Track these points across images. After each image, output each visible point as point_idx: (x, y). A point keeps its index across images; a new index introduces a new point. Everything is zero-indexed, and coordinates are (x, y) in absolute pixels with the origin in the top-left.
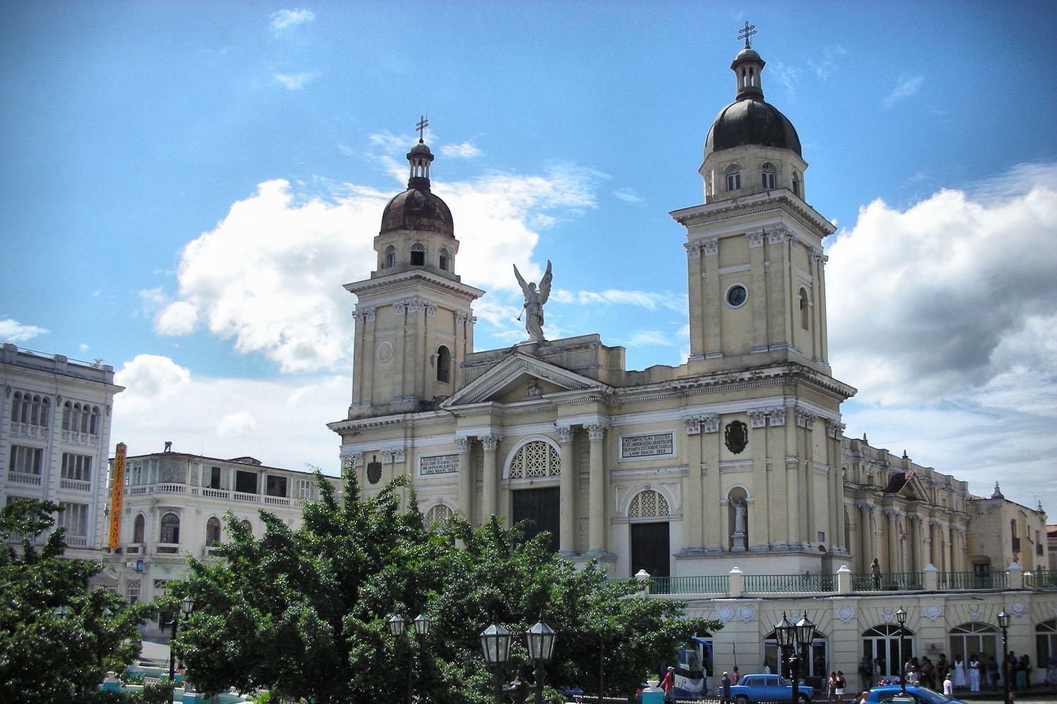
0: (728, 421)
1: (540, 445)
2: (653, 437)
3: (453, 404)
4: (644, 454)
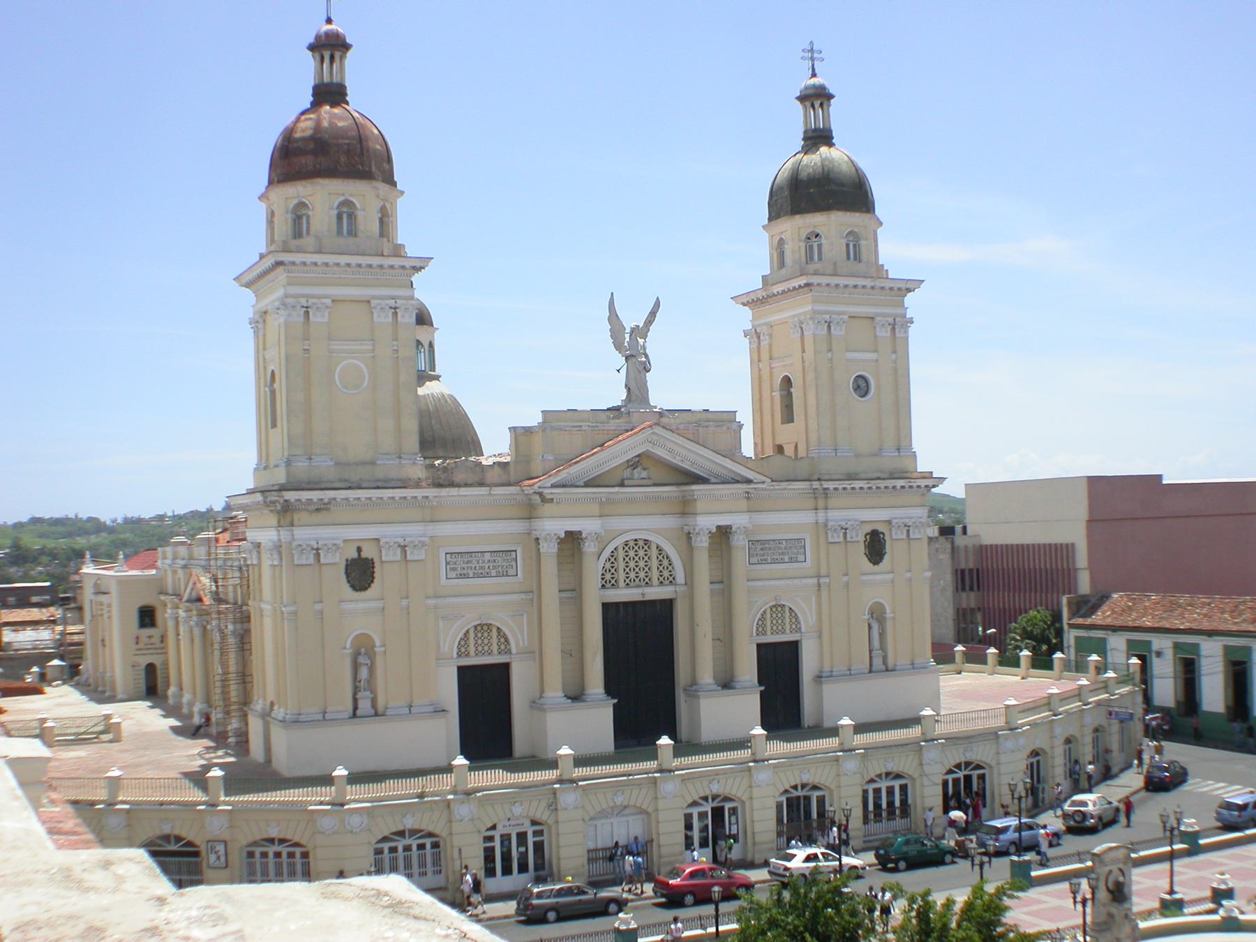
0: (868, 529)
1: (641, 543)
2: (784, 542)
3: (553, 486)
4: (774, 562)
